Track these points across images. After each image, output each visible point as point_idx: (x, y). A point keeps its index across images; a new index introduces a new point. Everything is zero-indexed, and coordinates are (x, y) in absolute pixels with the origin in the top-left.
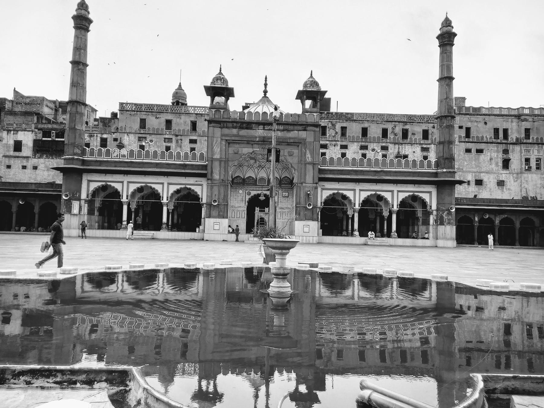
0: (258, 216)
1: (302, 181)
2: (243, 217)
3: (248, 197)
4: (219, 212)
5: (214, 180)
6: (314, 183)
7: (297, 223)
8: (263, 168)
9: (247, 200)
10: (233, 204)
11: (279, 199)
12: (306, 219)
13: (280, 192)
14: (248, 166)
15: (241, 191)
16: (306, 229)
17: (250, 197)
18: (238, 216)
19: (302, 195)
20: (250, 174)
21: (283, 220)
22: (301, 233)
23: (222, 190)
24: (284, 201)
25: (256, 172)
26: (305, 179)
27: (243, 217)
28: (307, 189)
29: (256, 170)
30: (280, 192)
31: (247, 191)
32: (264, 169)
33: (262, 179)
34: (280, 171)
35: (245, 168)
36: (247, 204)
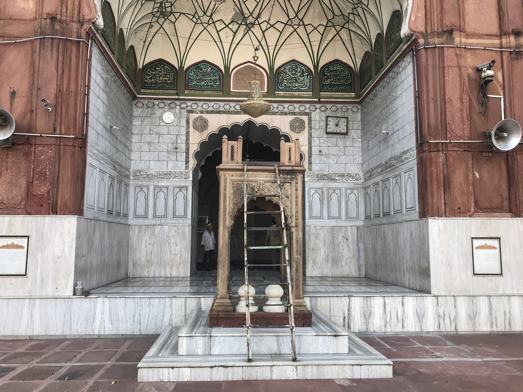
0: (238, 190)
1: (450, 20)
2: (180, 211)
3: (196, 139)
4: (30, 184)
5: (12, 19)
6: (502, 33)
7: (436, 226)
8: (249, 27)
9: (194, 148)
10: (142, 166)
11: (315, 142)
12: (484, 208)
13: (316, 115)
14: (195, 18)
15: (168, 117)
16: (486, 260)
17: (204, 136)
18: (160, 211)
19: (454, 90)
20: (204, 51)
21: (333, 223)
22: (462, 279)
23: (49, 68)
24: (334, 150)
25: (226, 47)
26: (460, 13)
27: (180, 211)
28: (470, 61)
29: (226, 36)
30: (316, 115)
31: (193, 116)
32: (256, 30)
33: (249, 70)
34: (316, 37)
35: (184, 25)
36: (193, 162)
